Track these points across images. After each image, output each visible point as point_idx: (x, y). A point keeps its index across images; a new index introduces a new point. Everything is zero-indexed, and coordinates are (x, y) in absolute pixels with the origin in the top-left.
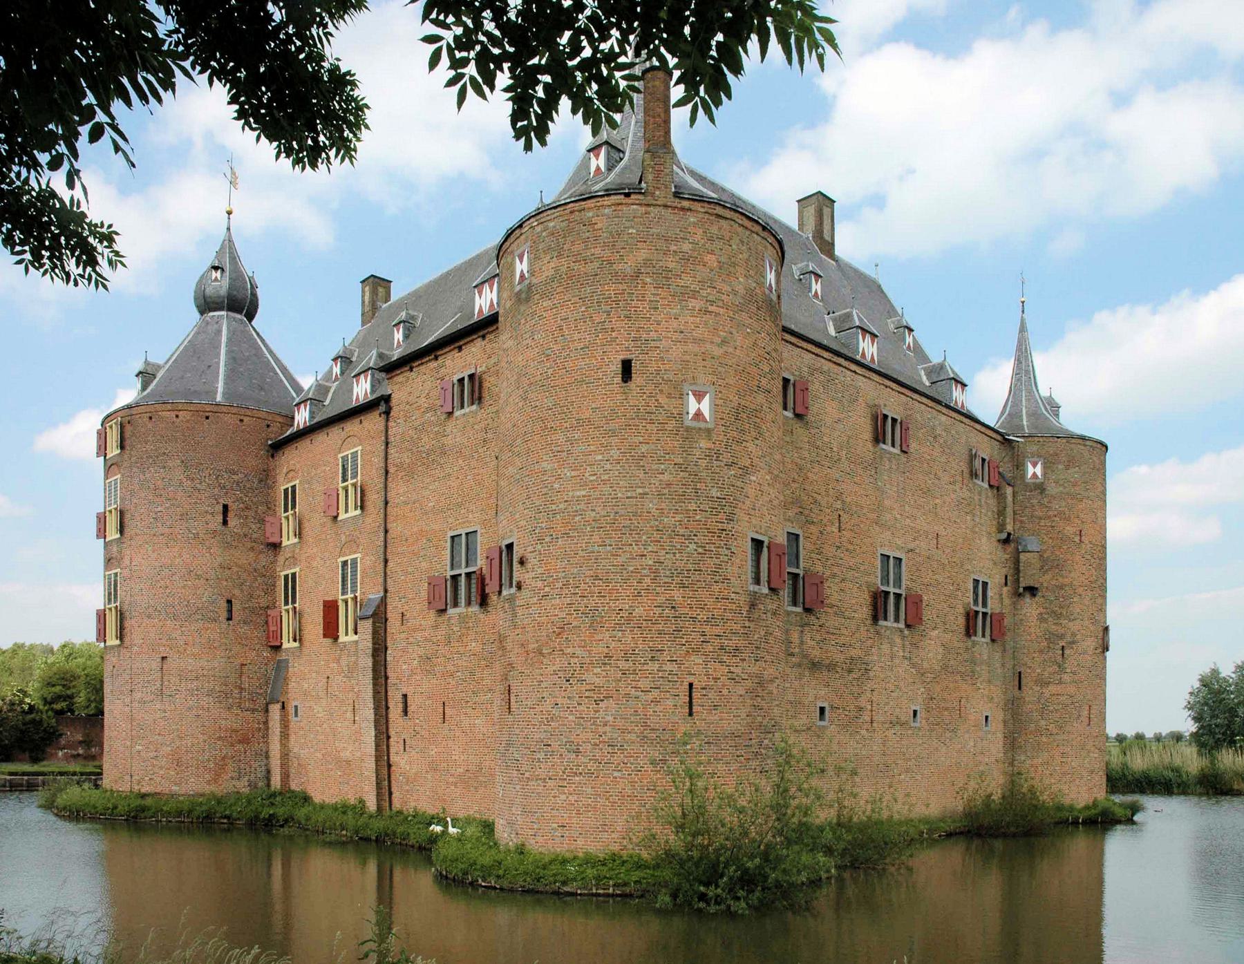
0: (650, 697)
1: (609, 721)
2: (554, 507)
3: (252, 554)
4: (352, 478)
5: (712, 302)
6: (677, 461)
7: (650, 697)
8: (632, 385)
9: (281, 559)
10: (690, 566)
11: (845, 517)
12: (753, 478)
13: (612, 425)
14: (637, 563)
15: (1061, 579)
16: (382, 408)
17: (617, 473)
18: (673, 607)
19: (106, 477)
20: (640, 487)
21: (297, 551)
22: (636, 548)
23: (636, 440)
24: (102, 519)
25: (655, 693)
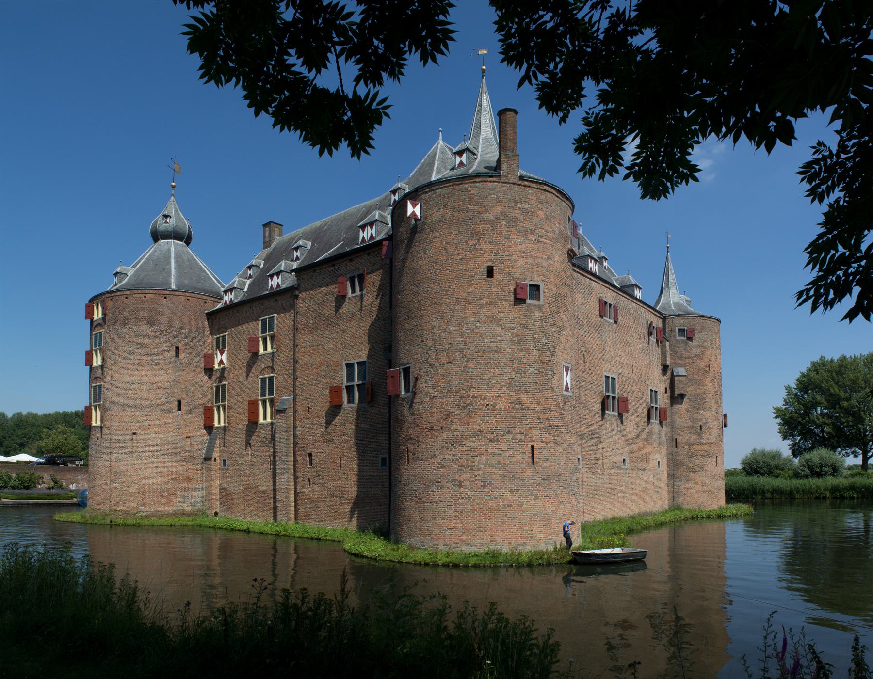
0: (508, 454)
1: (481, 468)
2: (441, 347)
5: (542, 237)
6: (521, 322)
7: (508, 454)
8: (493, 280)
11: (587, 356)
12: (564, 333)
14: (498, 378)
15: (698, 390)
17: (484, 328)
18: (521, 404)
20: (499, 336)
22: (497, 370)
25: (511, 452)
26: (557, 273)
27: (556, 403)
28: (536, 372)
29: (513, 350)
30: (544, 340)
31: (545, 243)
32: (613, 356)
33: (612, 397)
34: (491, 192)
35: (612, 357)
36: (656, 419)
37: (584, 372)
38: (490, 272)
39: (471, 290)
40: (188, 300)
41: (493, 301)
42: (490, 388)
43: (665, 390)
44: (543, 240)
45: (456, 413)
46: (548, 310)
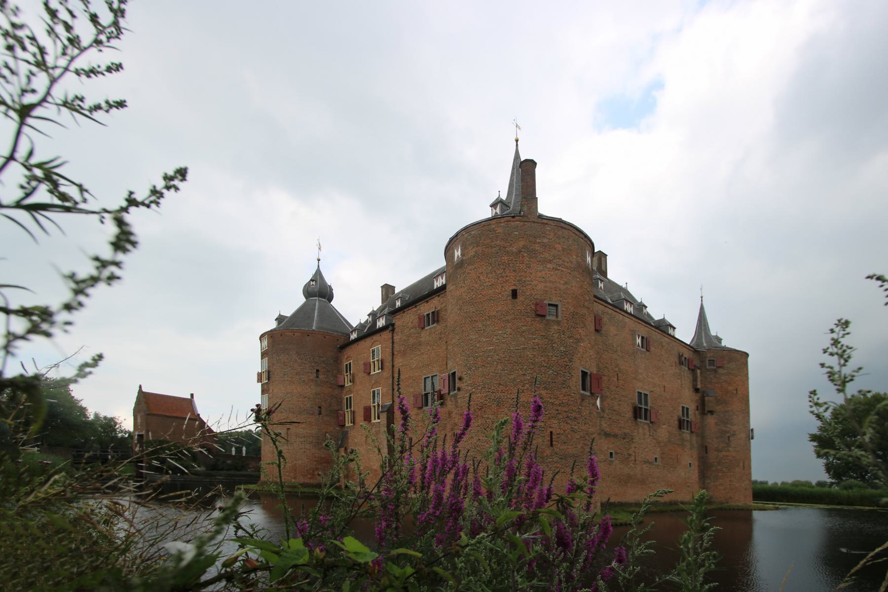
3: (330, 389)
4: (377, 357)
9: (344, 392)
10: (549, 380)
13: (509, 318)
16: (390, 328)
17: (510, 339)
19: (262, 359)
21: (352, 388)
23: (520, 324)
24: (260, 376)
26: (574, 296)
27: (573, 399)
28: (555, 373)
29: (534, 356)
30: (562, 348)
31: (562, 271)
32: (646, 377)
33: (645, 409)
34: (514, 230)
35: (644, 378)
36: (687, 430)
37: (617, 387)
38: (514, 294)
39: (499, 309)
40: (325, 337)
41: (517, 317)
42: (515, 385)
43: (696, 408)
44: (560, 268)
45: (488, 405)
46: (565, 325)
